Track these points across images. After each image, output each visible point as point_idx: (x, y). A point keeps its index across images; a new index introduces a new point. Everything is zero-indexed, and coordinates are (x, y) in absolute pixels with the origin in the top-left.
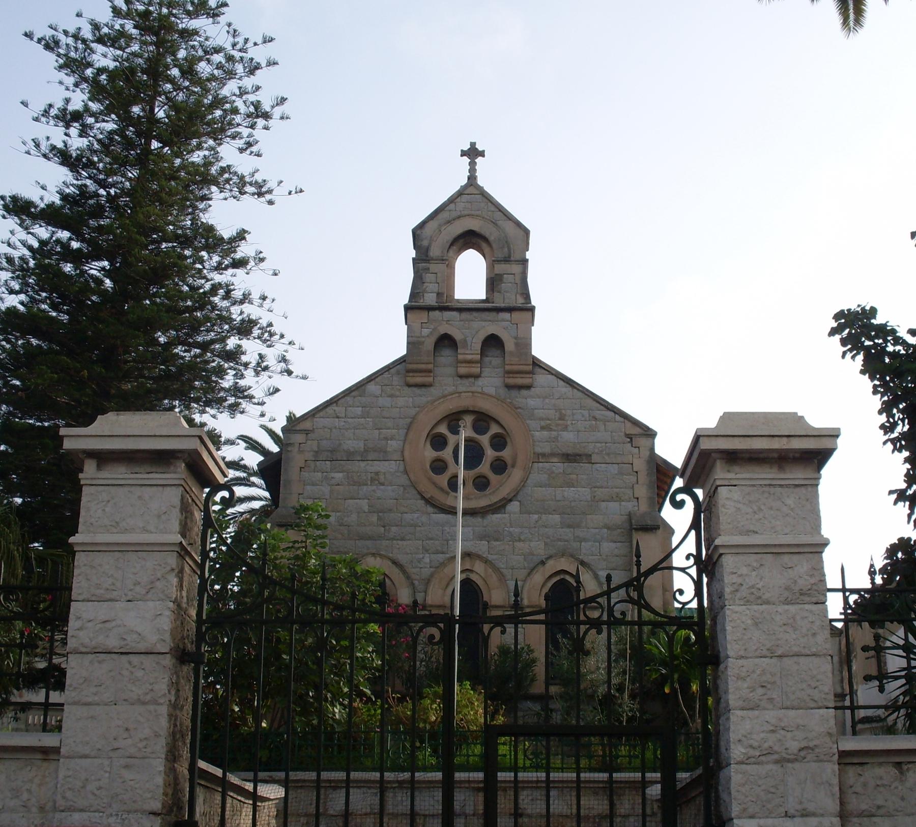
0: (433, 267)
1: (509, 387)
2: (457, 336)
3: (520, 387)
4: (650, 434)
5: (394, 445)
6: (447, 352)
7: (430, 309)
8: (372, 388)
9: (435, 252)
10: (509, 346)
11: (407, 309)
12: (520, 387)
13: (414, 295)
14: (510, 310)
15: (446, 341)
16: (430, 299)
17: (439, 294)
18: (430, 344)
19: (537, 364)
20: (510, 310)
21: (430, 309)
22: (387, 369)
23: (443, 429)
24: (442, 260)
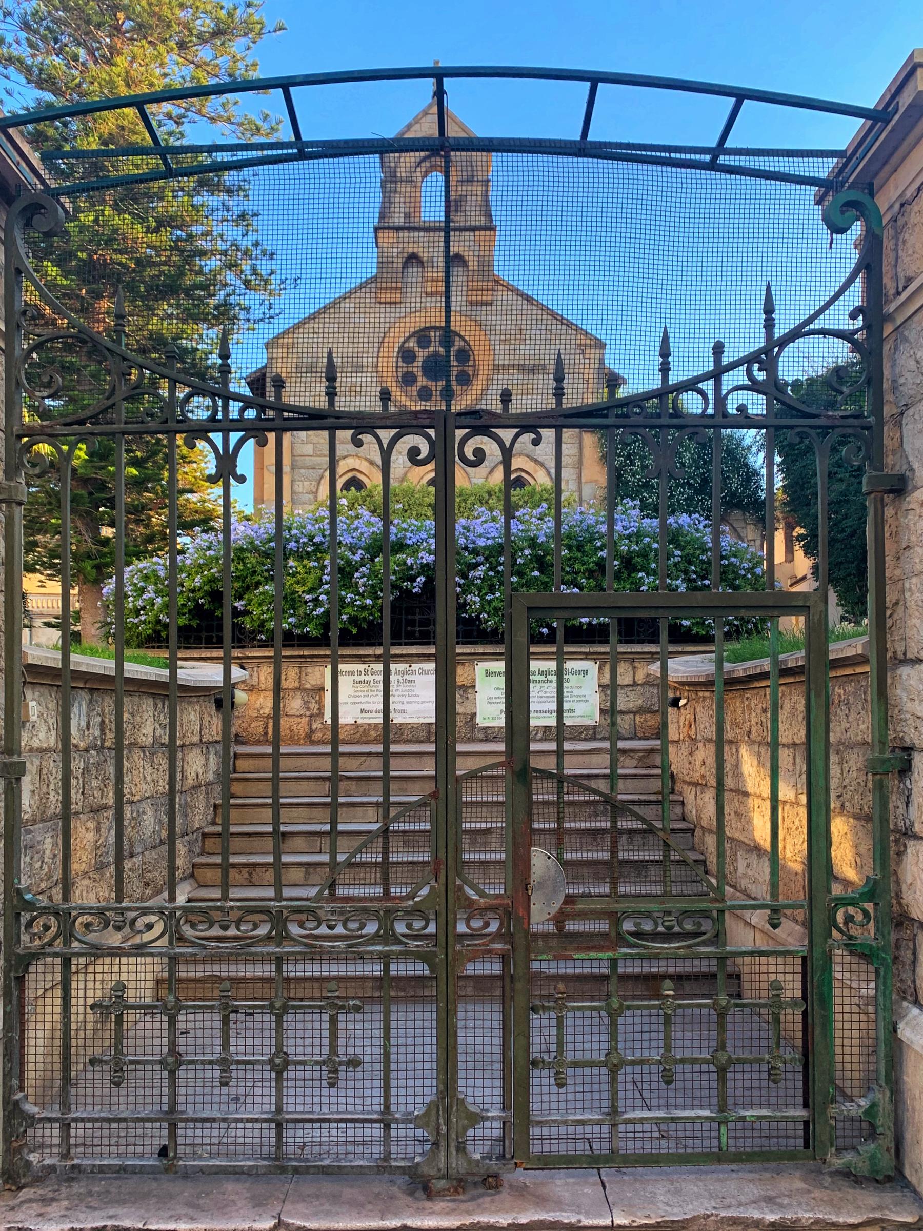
0: (401, 188)
1: (471, 303)
2: (425, 256)
3: (483, 304)
4: (601, 345)
5: (368, 360)
6: (414, 270)
7: (398, 229)
8: (347, 305)
9: (402, 173)
10: (473, 264)
11: (376, 230)
12: (483, 304)
13: (382, 216)
14: (473, 229)
15: (413, 259)
16: (398, 219)
17: (407, 216)
18: (399, 263)
19: (497, 282)
20: (473, 229)
21: (398, 229)
22: (361, 286)
23: (412, 344)
24: (409, 180)
